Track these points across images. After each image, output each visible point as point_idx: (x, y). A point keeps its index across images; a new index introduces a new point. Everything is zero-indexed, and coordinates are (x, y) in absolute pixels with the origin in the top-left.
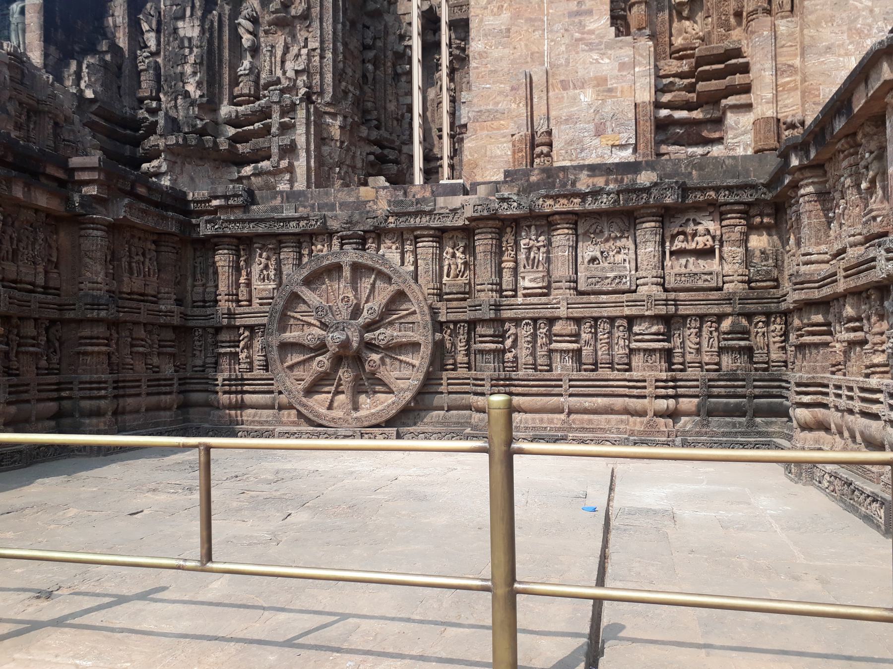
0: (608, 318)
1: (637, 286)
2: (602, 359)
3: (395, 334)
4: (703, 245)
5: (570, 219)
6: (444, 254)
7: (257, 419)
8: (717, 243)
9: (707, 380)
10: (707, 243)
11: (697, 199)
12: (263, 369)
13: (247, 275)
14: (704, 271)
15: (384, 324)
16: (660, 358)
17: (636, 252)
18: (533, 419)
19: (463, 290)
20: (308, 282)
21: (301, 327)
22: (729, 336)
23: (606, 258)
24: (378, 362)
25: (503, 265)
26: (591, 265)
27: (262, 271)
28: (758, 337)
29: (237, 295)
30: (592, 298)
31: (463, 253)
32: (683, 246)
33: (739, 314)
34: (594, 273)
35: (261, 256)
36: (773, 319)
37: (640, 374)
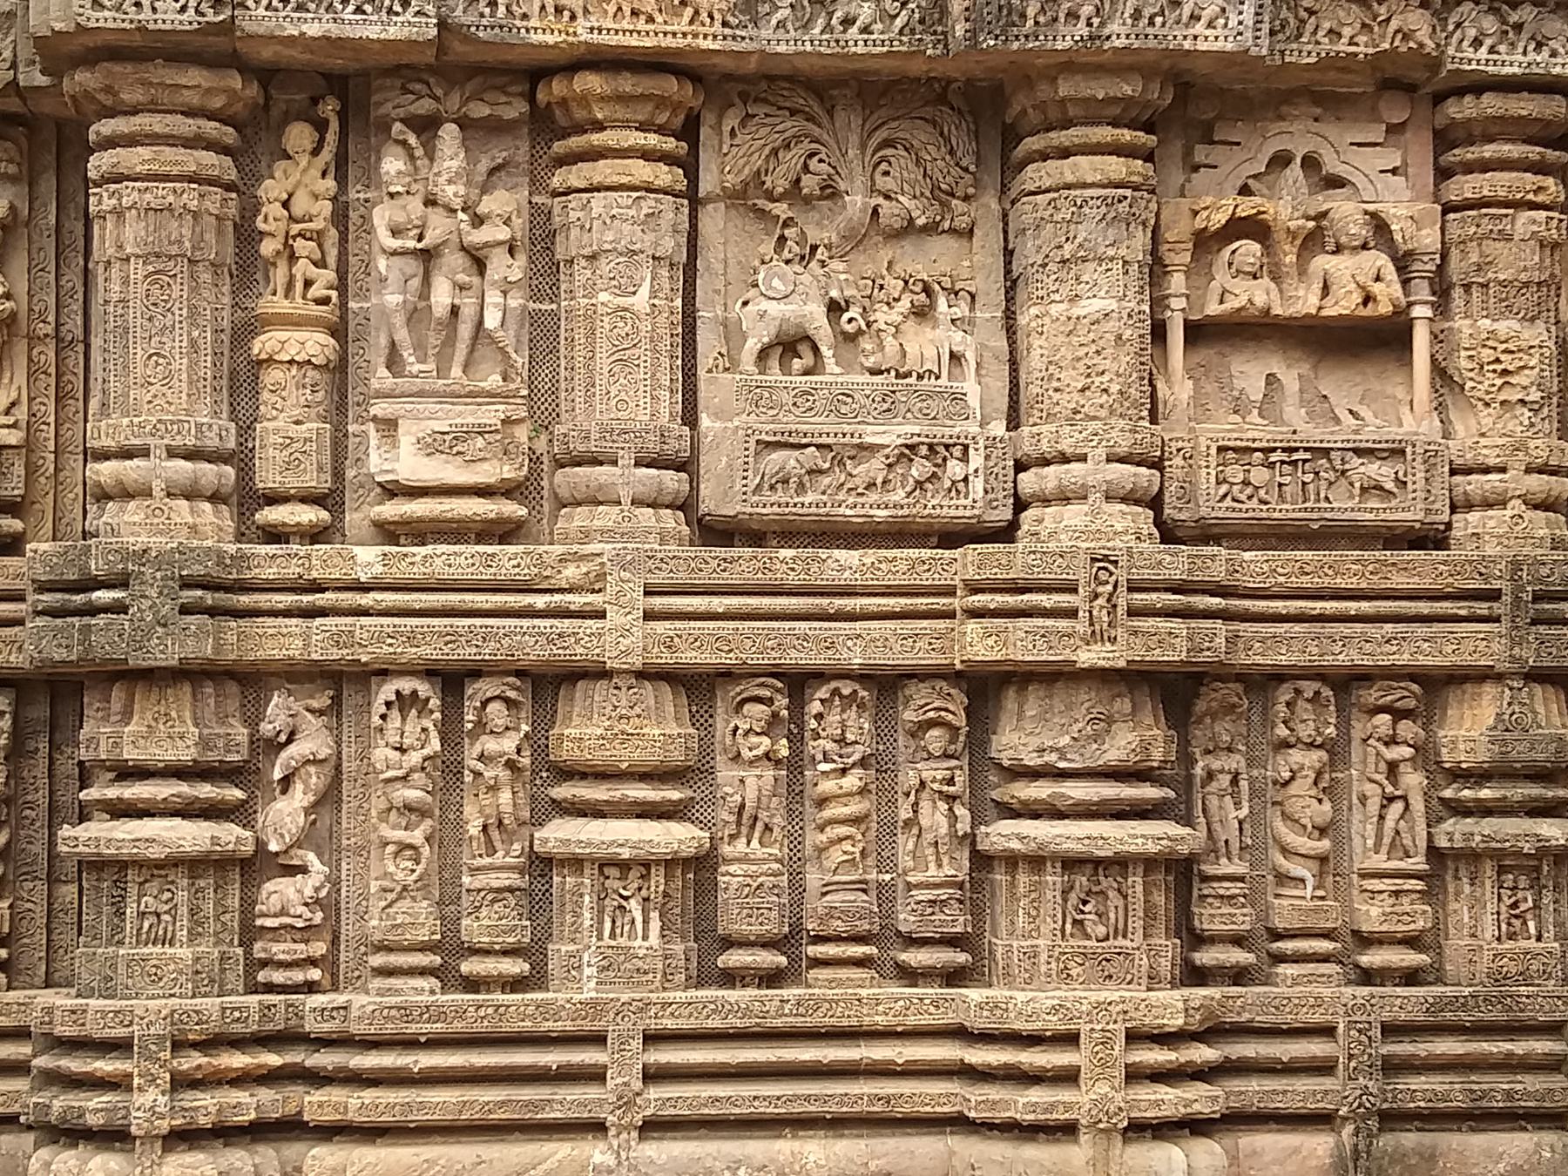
0: (865, 677)
2: (831, 912)
4: (1357, 298)
5: (661, 102)
8: (1422, 291)
9: (1376, 1033)
10: (1377, 288)
14: (1367, 437)
17: (1010, 316)
22: (1485, 793)
23: (852, 338)
26: (775, 375)
30: (785, 561)
32: (1260, 300)
33: (1535, 676)
34: (791, 422)
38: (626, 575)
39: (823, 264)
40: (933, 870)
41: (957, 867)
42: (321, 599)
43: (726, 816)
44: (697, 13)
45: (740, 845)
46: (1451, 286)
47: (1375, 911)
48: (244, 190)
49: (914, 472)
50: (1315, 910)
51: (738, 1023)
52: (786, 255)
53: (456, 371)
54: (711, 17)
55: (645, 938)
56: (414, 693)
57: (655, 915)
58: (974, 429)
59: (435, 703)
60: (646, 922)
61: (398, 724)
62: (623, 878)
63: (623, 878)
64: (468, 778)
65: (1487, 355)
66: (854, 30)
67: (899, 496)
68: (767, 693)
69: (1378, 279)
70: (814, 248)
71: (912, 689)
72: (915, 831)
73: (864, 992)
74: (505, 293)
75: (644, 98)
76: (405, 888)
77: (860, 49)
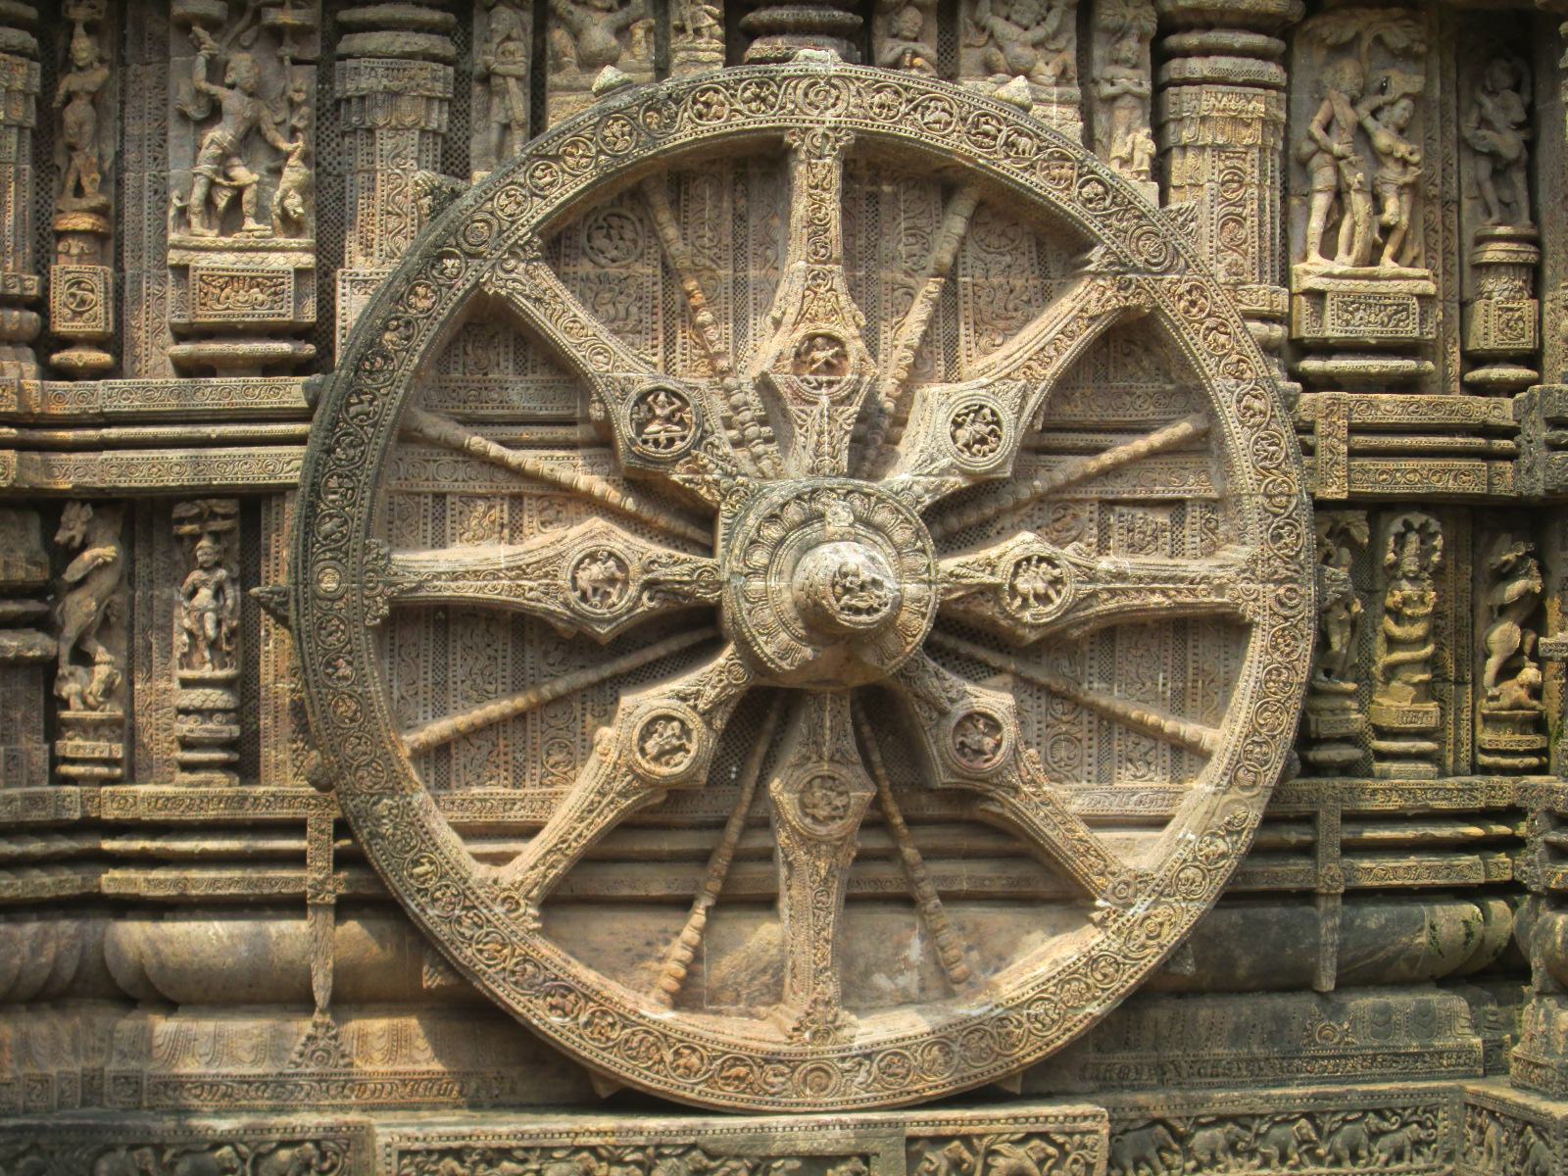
3: (1104, 564)
13: (104, 180)
15: (1018, 505)
19: (1410, 330)
21: (501, 512)
24: (1010, 732)
27: (223, 160)
29: (40, 304)
35: (216, 70)
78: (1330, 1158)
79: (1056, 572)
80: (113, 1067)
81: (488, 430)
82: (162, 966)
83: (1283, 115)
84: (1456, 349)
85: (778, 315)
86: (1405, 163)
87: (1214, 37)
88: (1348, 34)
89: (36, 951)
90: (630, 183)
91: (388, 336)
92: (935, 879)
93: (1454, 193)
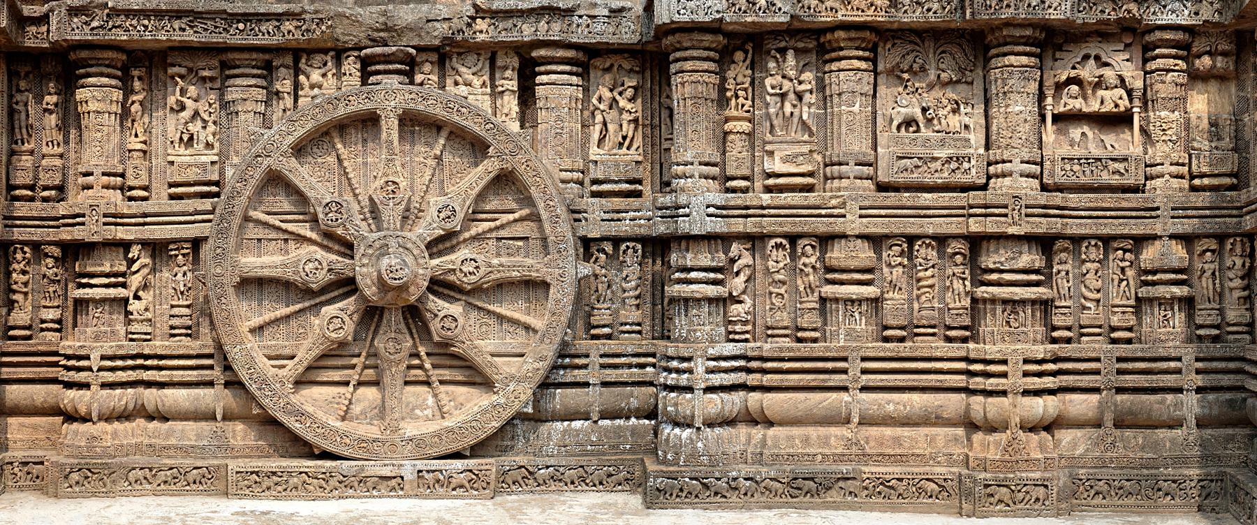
0: (934, 237)
1: (989, 178)
3: (495, 261)
4: (1113, 105)
5: (863, 40)
6: (594, 101)
7: (173, 441)
8: (1137, 102)
10: (1119, 102)
11: (1105, 16)
12: (187, 335)
14: (1115, 154)
15: (465, 240)
16: (1033, 315)
17: (986, 111)
18: (790, 438)
20: (299, 150)
25: (729, 126)
28: (1204, 279)
31: (632, 100)
32: (1078, 106)
34: (909, 149)
36: (1229, 247)
37: (995, 348)
38: (853, 203)
39: (920, 95)
40: (958, 303)
41: (967, 302)
42: (750, 212)
43: (885, 284)
44: (876, 8)
45: (891, 294)
46: (1148, 101)
47: (1115, 319)
48: (721, 74)
49: (951, 167)
50: (1095, 318)
51: (889, 354)
52: (907, 91)
53: (793, 134)
54: (881, 9)
55: (860, 325)
56: (781, 243)
57: (863, 318)
58: (972, 151)
59: (788, 246)
60: (861, 319)
61: (775, 253)
62: (852, 305)
63: (852, 305)
64: (798, 271)
65: (1158, 124)
66: (931, 13)
67: (946, 175)
68: (900, 243)
69: (1121, 98)
70: (917, 89)
71: (950, 240)
72: (951, 290)
73: (933, 345)
74: (809, 108)
75: (858, 38)
76: (779, 308)
77: (933, 20)
78: (591, 484)
79: (477, 264)
80: (146, 441)
81: (275, 216)
82: (164, 405)
83: (581, 96)
84: (658, 181)
85: (375, 174)
86: (631, 113)
87: (549, 67)
88: (607, 65)
89: (120, 400)
90: (325, 129)
91: (239, 184)
92: (437, 375)
93: (658, 123)
